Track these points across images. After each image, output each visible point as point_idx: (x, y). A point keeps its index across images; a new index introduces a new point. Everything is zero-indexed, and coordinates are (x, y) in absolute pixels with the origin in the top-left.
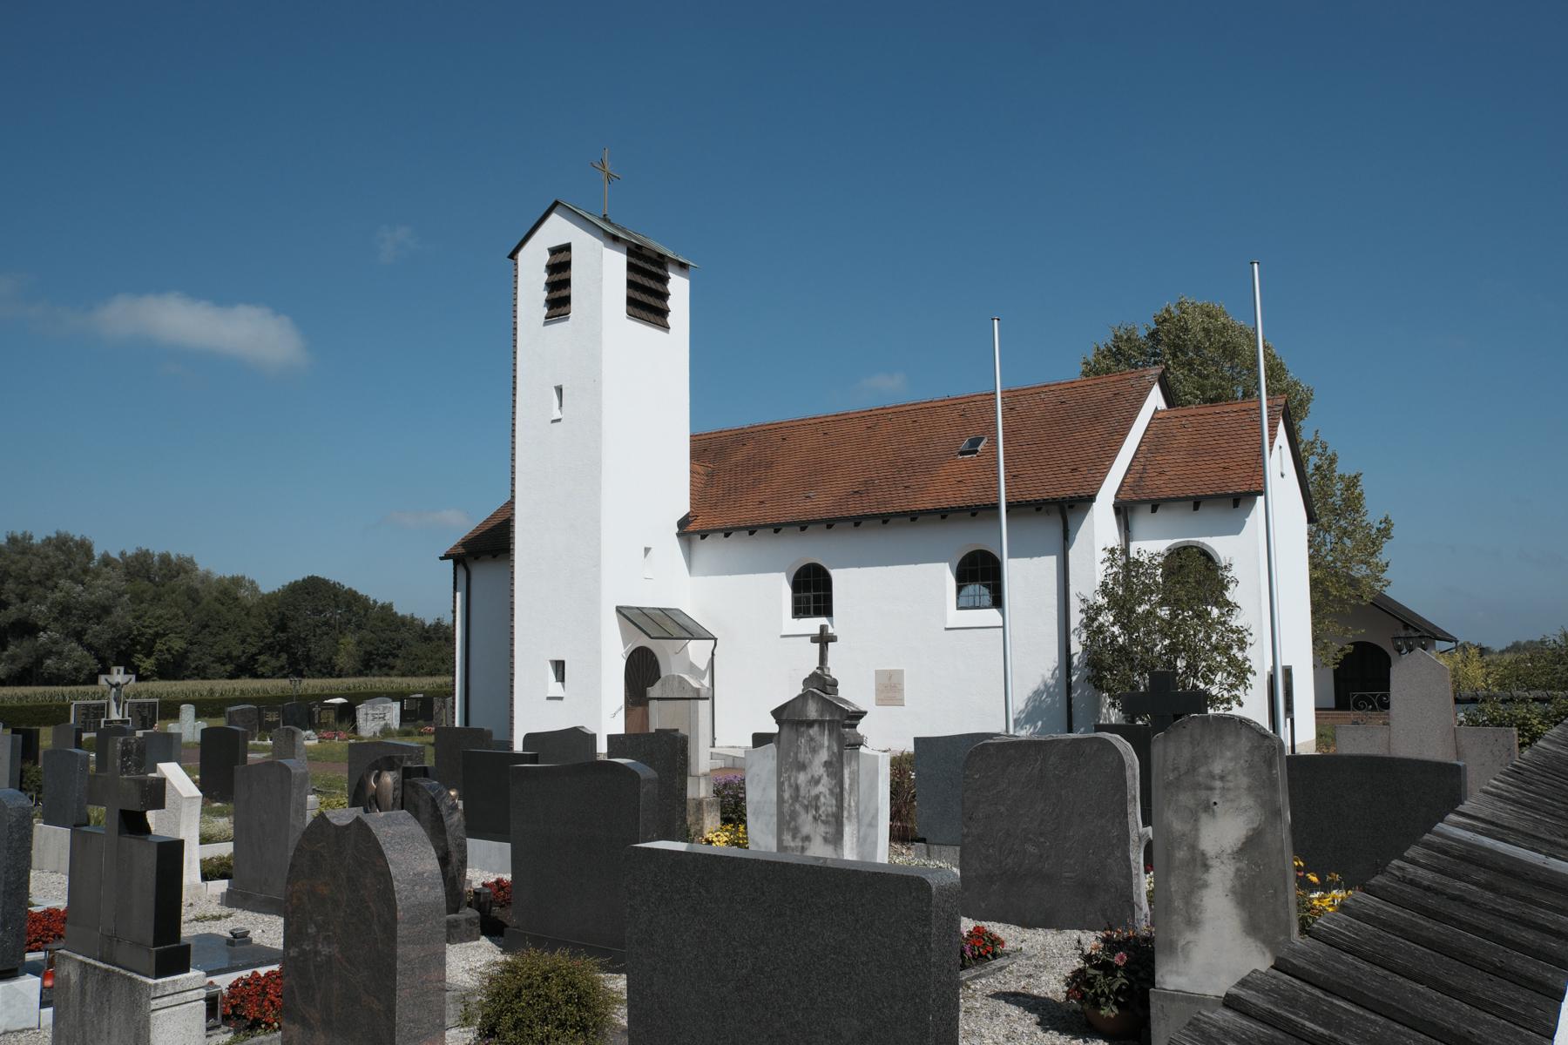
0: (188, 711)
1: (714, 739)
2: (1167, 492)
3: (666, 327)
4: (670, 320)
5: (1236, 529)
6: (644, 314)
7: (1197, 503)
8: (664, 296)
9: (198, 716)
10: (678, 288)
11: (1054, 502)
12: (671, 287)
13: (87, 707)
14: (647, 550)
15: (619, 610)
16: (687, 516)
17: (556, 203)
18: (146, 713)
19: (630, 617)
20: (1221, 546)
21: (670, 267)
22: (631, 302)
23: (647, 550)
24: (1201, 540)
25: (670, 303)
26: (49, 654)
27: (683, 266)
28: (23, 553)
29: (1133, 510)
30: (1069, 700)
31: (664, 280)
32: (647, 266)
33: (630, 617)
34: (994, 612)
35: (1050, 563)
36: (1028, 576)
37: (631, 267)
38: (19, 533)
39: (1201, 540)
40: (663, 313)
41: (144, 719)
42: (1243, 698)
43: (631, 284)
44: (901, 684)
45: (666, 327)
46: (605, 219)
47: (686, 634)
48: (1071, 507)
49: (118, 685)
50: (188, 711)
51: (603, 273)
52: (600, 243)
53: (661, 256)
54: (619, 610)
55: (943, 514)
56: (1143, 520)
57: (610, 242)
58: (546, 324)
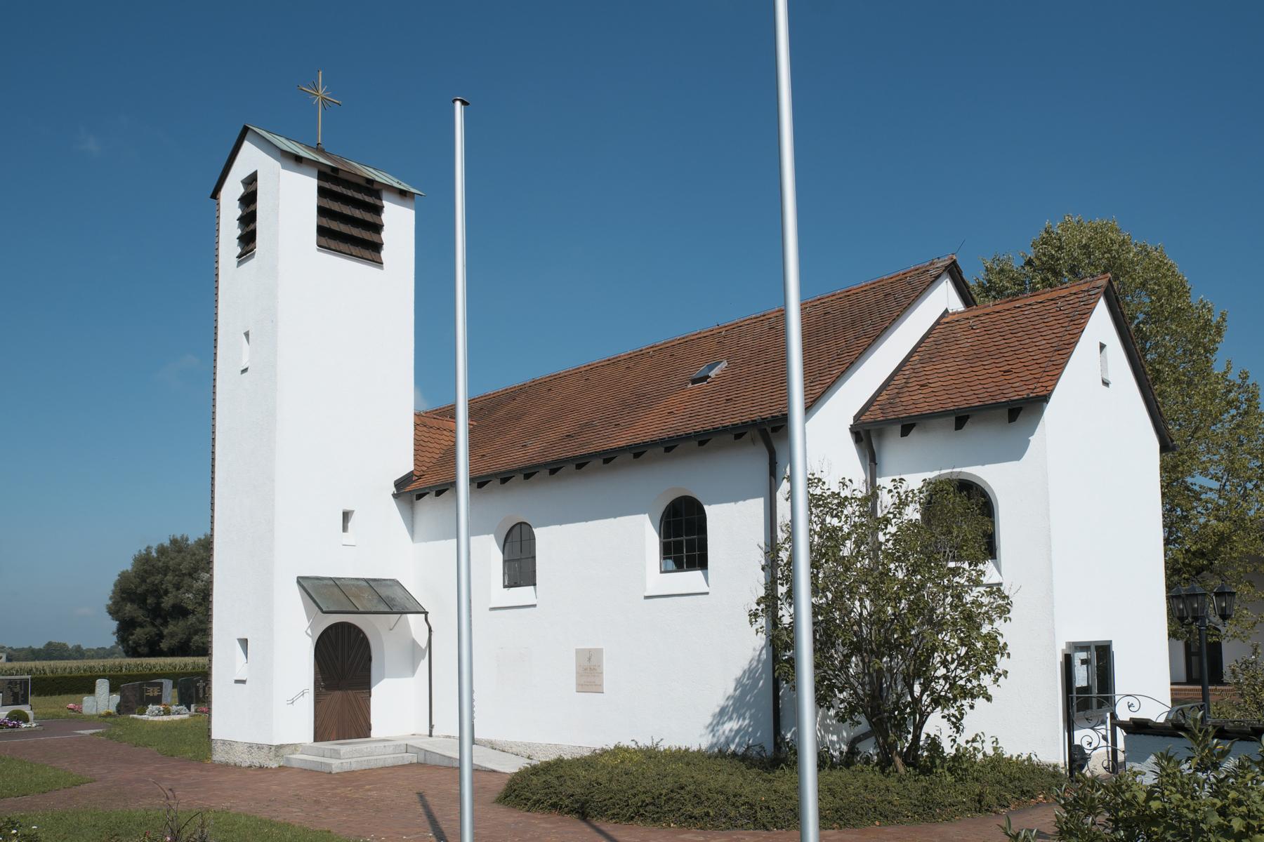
0: (102, 686)
2: (925, 408)
3: (379, 263)
4: (384, 254)
5: (1017, 452)
6: (343, 247)
7: (961, 419)
8: (378, 228)
9: (113, 690)
10: (398, 222)
11: (754, 424)
14: (346, 516)
15: (301, 581)
19: (316, 590)
20: (993, 476)
21: (385, 195)
22: (321, 231)
23: (346, 516)
25: (385, 236)
26: (196, 632)
27: (403, 194)
28: (180, 551)
29: (881, 434)
31: (378, 210)
32: (350, 193)
34: (697, 574)
35: (756, 506)
36: (734, 527)
37: (322, 192)
38: (178, 536)
40: (377, 247)
41: (15, 695)
43: (322, 211)
45: (379, 263)
46: (319, 150)
48: (775, 430)
50: (102, 686)
51: (292, 199)
52: (278, 164)
53: (370, 181)
54: (301, 581)
55: (638, 452)
56: (894, 450)
57: (292, 163)
58: (239, 264)
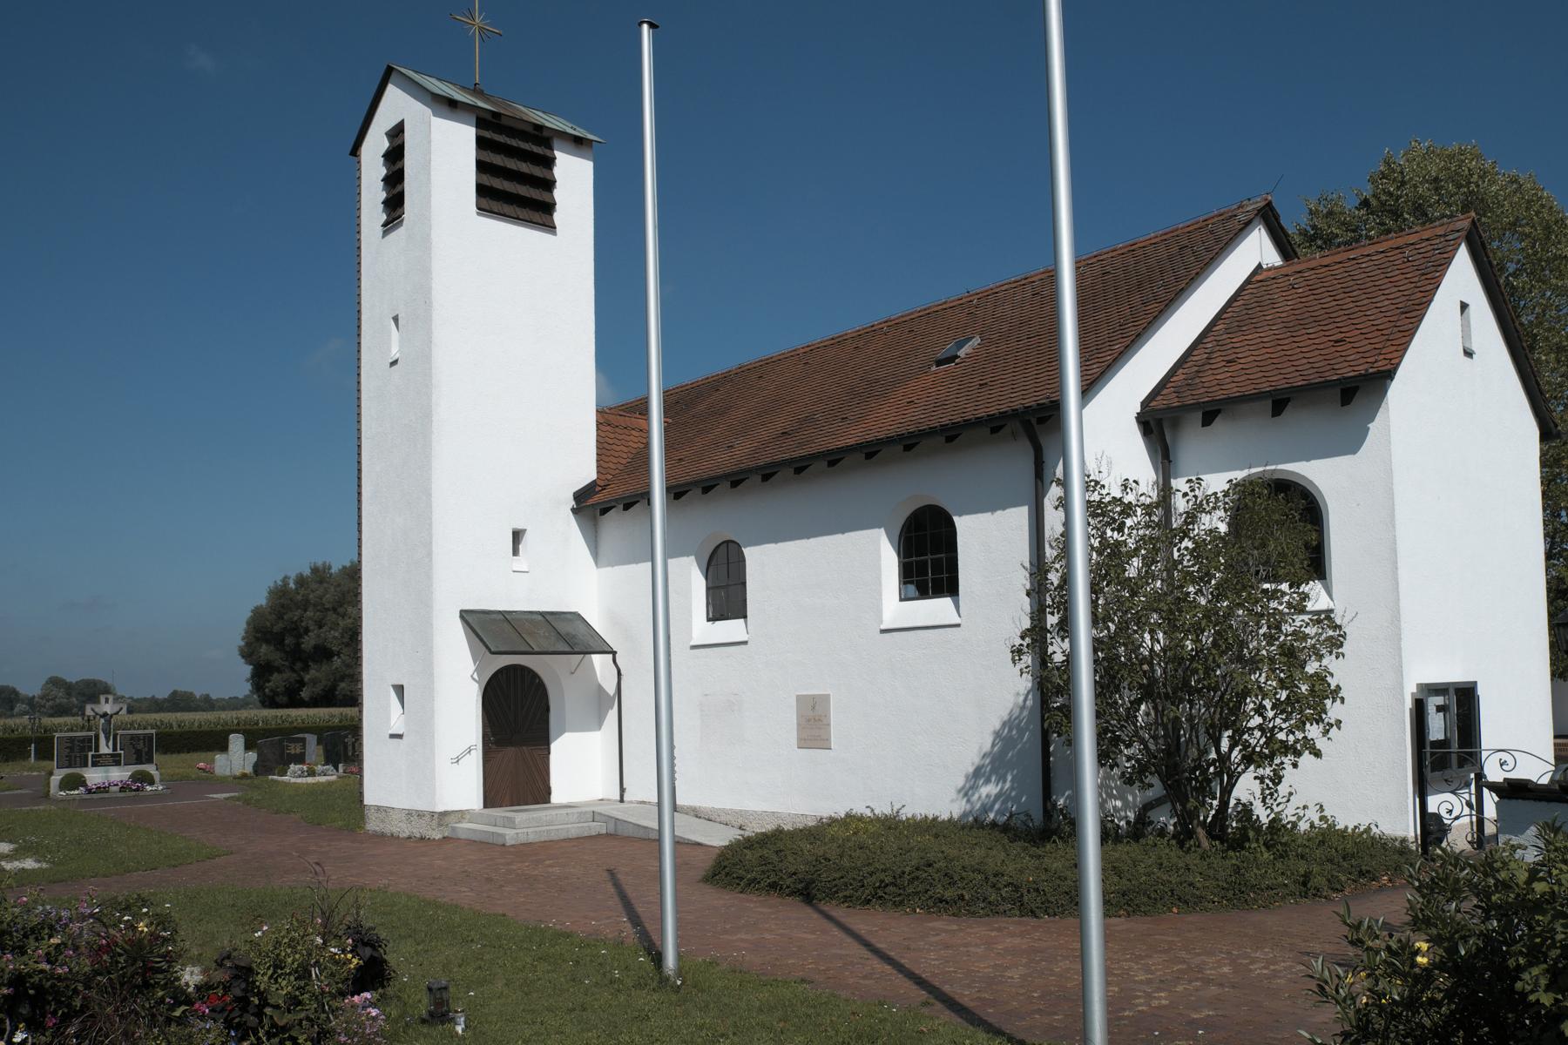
0: (236, 742)
1: (622, 790)
2: (1233, 390)
3: (550, 227)
4: (558, 217)
5: (1352, 443)
6: (507, 209)
7: (1279, 403)
8: (549, 184)
9: (248, 747)
10: (573, 178)
11: (1014, 415)
12: (558, 172)
13: (71, 739)
14: (517, 536)
15: (466, 616)
16: (592, 485)
17: (389, 71)
18: (140, 746)
19: (483, 627)
20: (1322, 474)
21: (556, 143)
22: (482, 190)
23: (517, 536)
24: (1280, 467)
25: (558, 194)
26: (342, 679)
27: (578, 144)
28: (321, 582)
29: (1176, 424)
30: (1046, 754)
31: (549, 162)
32: (514, 142)
33: (481, 625)
34: (946, 602)
35: (1019, 517)
36: (990, 542)
37: (481, 143)
38: (320, 564)
39: (1280, 467)
40: (548, 208)
41: (138, 752)
42: (1321, 744)
43: (482, 166)
44: (827, 716)
45: (550, 227)
46: (477, 91)
47: (562, 647)
48: (1041, 421)
49: (105, 715)
50: (236, 742)
51: (447, 153)
52: (429, 111)
53: (539, 128)
54: (466, 616)
55: (870, 452)
56: (1193, 443)
57: (446, 109)
58: (385, 233)
